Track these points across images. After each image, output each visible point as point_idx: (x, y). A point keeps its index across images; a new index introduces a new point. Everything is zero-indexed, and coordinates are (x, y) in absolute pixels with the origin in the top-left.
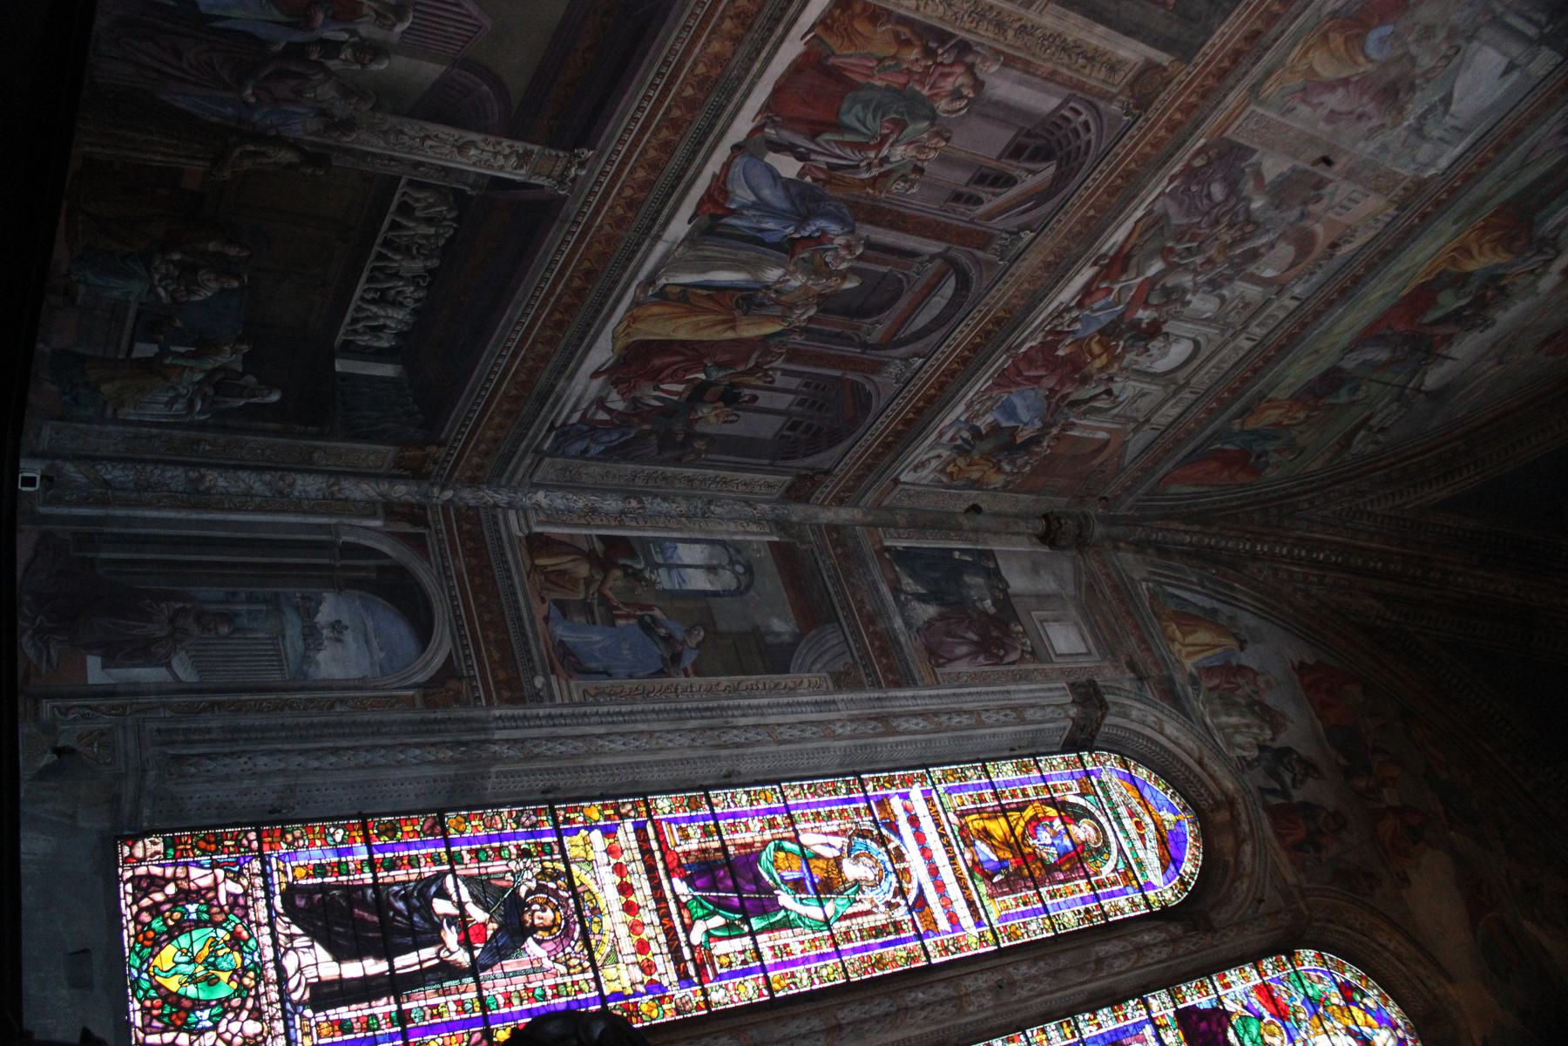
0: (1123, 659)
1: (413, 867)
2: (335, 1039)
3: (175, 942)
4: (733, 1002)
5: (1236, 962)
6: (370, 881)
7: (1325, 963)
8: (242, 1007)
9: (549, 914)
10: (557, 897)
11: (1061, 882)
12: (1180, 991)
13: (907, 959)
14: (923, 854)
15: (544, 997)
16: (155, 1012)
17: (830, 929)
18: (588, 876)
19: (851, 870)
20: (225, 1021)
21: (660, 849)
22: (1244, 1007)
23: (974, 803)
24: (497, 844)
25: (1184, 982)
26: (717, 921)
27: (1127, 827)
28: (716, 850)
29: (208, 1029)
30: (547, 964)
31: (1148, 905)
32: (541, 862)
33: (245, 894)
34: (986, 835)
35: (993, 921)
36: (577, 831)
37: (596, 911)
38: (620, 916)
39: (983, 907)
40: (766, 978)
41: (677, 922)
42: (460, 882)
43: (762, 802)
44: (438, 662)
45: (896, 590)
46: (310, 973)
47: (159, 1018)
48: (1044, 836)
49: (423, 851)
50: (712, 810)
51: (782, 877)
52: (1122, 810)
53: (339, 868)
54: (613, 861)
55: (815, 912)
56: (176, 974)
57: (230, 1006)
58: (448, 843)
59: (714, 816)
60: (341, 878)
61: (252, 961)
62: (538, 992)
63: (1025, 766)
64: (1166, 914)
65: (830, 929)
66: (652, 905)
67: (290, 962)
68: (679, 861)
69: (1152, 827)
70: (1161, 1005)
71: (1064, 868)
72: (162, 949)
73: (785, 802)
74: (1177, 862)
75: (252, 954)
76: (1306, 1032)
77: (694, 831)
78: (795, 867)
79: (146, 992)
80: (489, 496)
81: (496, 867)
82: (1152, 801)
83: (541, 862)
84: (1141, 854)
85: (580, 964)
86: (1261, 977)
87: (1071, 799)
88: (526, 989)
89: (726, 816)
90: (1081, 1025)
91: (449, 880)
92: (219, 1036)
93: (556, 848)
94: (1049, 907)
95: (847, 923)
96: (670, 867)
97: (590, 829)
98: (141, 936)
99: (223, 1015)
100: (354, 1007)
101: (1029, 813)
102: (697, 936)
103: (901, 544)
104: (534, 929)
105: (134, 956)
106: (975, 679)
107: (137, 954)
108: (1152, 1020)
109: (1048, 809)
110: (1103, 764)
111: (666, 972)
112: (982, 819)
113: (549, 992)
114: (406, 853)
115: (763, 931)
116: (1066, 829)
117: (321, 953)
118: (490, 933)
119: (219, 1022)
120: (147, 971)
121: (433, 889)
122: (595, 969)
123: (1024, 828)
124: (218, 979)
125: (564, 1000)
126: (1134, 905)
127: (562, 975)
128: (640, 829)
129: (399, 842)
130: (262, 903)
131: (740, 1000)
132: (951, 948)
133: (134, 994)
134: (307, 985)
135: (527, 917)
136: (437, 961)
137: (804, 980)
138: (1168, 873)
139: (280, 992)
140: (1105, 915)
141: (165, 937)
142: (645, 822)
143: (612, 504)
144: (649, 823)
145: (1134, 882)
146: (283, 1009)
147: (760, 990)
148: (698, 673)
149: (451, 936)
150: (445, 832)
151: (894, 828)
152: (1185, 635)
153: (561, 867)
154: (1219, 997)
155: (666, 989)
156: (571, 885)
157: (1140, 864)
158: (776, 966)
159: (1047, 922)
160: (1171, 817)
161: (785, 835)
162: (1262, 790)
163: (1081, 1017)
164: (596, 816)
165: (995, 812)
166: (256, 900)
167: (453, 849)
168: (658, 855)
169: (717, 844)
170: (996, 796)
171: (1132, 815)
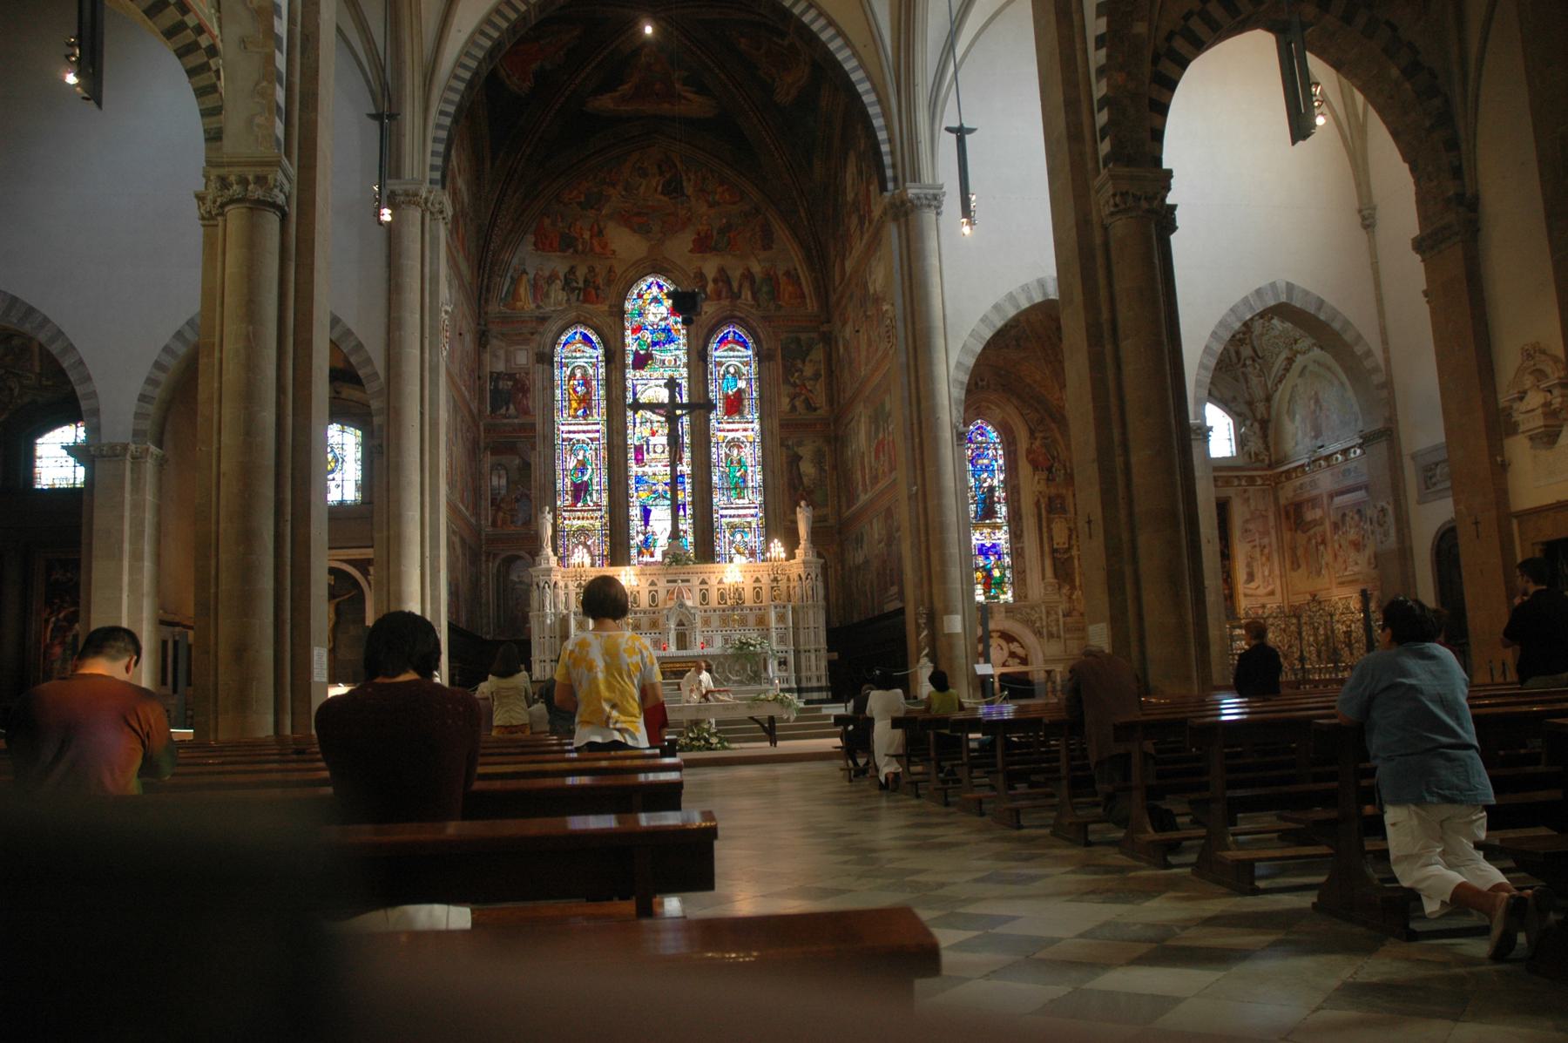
0: (529, 336)
19: (580, 457)
26: (588, 498)
34: (576, 410)
44: (527, 556)
45: (505, 417)
48: (579, 389)
52: (574, 354)
55: (589, 471)
70: (630, 373)
77: (567, 497)
80: (483, 537)
84: (588, 355)
87: (568, 373)
101: (571, 391)
102: (591, 504)
103: (489, 409)
106: (534, 401)
111: (598, 514)
137: (605, 479)
143: (483, 503)
148: (530, 490)
151: (571, 439)
152: (521, 300)
157: (591, 357)
160: (578, 335)
162: (578, 300)
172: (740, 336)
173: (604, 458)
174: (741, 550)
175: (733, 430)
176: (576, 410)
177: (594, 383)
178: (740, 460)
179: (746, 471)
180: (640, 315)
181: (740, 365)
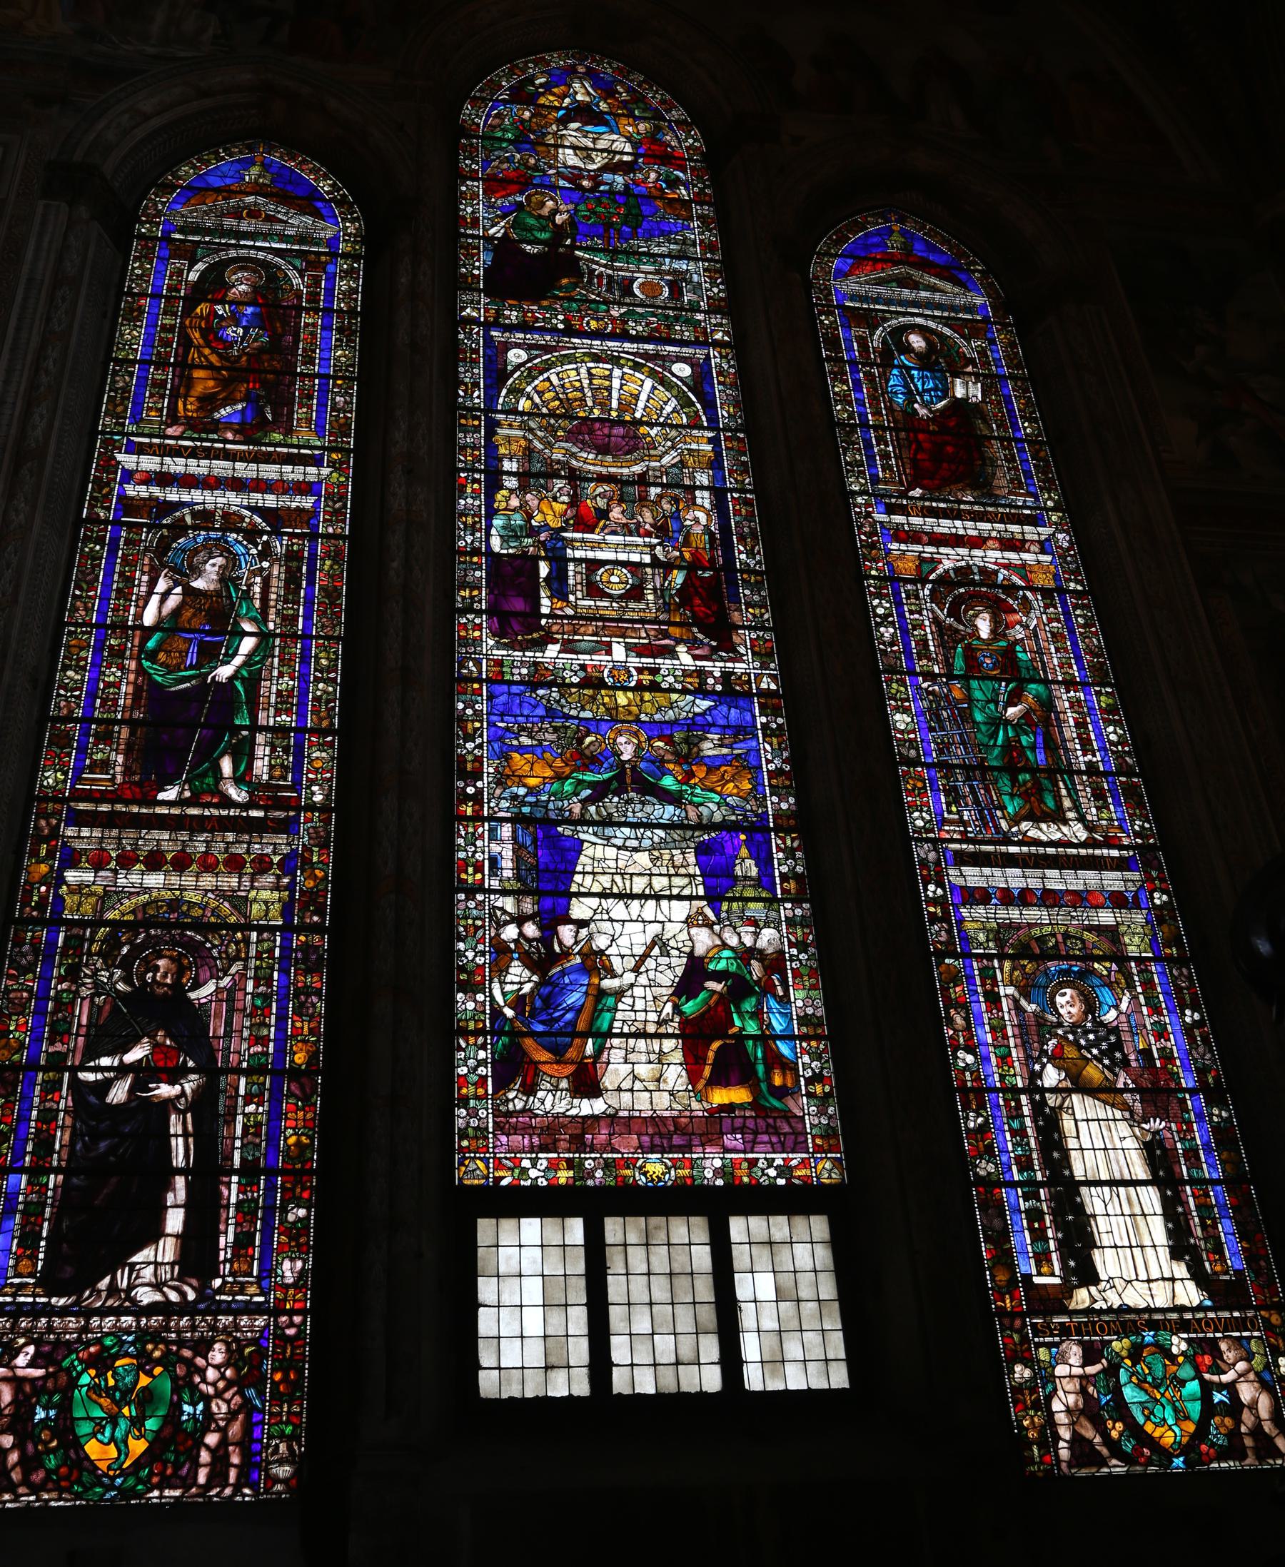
1: (56, 1119)
2: (256, 1256)
3: (83, 1441)
4: (330, 780)
5: (454, 198)
6: (60, 1177)
7: (484, 100)
8: (189, 1363)
9: (161, 963)
10: (143, 947)
11: (296, 341)
12: (464, 275)
13: (335, 562)
14: (212, 489)
15: (266, 997)
16: (169, 1471)
17: (276, 636)
18: (126, 901)
20: (203, 1387)
21: (113, 802)
22: (503, 218)
23: (163, 397)
24: (50, 1004)
25: (457, 267)
26: (226, 766)
27: (251, 229)
28: (132, 734)
29: (207, 1408)
30: (226, 982)
31: (355, 257)
32: (90, 954)
33: (38, 1343)
34: (209, 402)
35: (319, 444)
36: (59, 900)
37: (175, 904)
38: (188, 880)
39: (299, 447)
40: (312, 731)
41: (215, 812)
42: (92, 1064)
43: (83, 654)
46: (165, 1274)
47: (177, 1466)
48: (231, 332)
49: (37, 1100)
50: (76, 720)
51: (191, 667)
52: (229, 223)
53: (33, 1213)
54: (113, 865)
55: (248, 644)
56: (125, 1442)
57: (184, 1378)
58: (33, 1066)
59: (87, 720)
60: (47, 1215)
61: (132, 1343)
62: (259, 1002)
63: (132, 311)
64: (366, 238)
65: (276, 636)
66: (184, 835)
67: (146, 1296)
68: (135, 783)
69: (261, 200)
71: (280, 330)
72: (87, 1457)
73: (92, 626)
74: (314, 194)
75: (125, 1342)
76: (551, 167)
78: (183, 647)
79: (139, 1481)
81: (82, 1014)
82: (228, 181)
83: (90, 954)
84: (290, 232)
85: (237, 943)
86: (478, 179)
87: (193, 276)
88: (251, 1015)
89: (90, 706)
90: (469, 404)
91: (82, 1076)
92: (219, 1394)
93: (75, 931)
94: (322, 371)
95: (273, 611)
96: (139, 796)
97: (61, 881)
98: (63, 1484)
99: (194, 1388)
100: (222, 1227)
102: (237, 794)
104: (178, 987)
105: (90, 1495)
107: (86, 1489)
108: (487, 326)
109: (198, 310)
110: (159, 214)
111: (274, 845)
112: (186, 396)
113: (262, 989)
114: (33, 1124)
115: (254, 717)
116: (231, 303)
117: (145, 1254)
118: (168, 1042)
119: (201, 1391)
120: (113, 1478)
121: (92, 1099)
122: (249, 927)
123: (214, 351)
124: (144, 1388)
125: (276, 975)
126: (349, 273)
127: (246, 968)
128: (78, 819)
129: (15, 1131)
130: (57, 1321)
131: (331, 771)
132: (337, 506)
133: (140, 1496)
134: (180, 1278)
135: (160, 991)
136: (189, 1115)
138: (324, 211)
139: (181, 1317)
140: (352, 313)
141: (72, 1454)
142: (69, 808)
144: (72, 804)
145: (323, 258)
146: (203, 1313)
147: (325, 743)
149: (165, 1090)
150: (16, 1067)
153: (102, 931)
154: (484, 237)
155: (294, 852)
156: (133, 927)
157: (301, 239)
158: (302, 716)
159: (339, 382)
160: (255, 171)
161: (136, 642)
163: (461, 400)
164: (43, 868)
165: (181, 377)
166: (50, 1329)
167: (42, 1062)
168: (119, 807)
169: (125, 733)
170: (162, 364)
171: (237, 214)
172: (933, 249)
173: (331, 594)
174: (1093, 1073)
175: (955, 541)
176: (209, 402)
177: (305, 319)
178: (1009, 652)
179: (1048, 705)
180: (529, 139)
181: (947, 331)
